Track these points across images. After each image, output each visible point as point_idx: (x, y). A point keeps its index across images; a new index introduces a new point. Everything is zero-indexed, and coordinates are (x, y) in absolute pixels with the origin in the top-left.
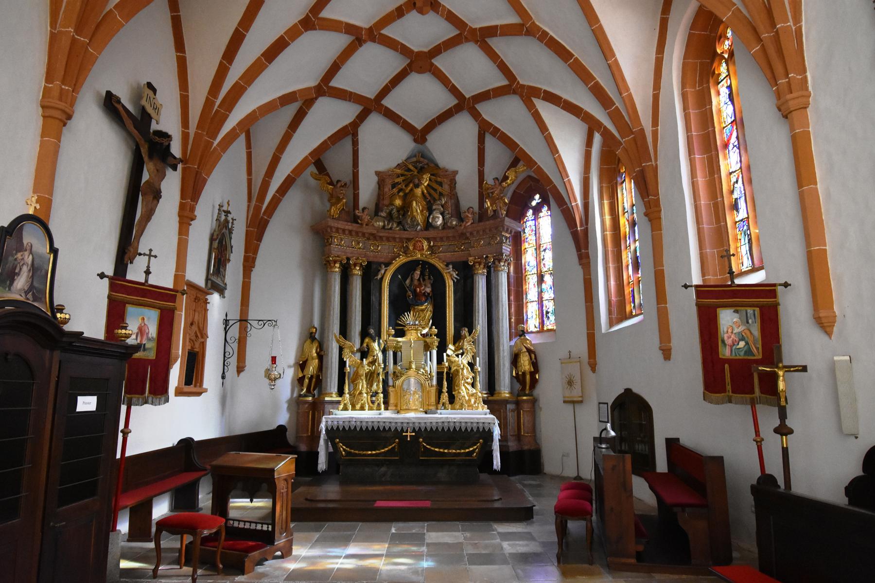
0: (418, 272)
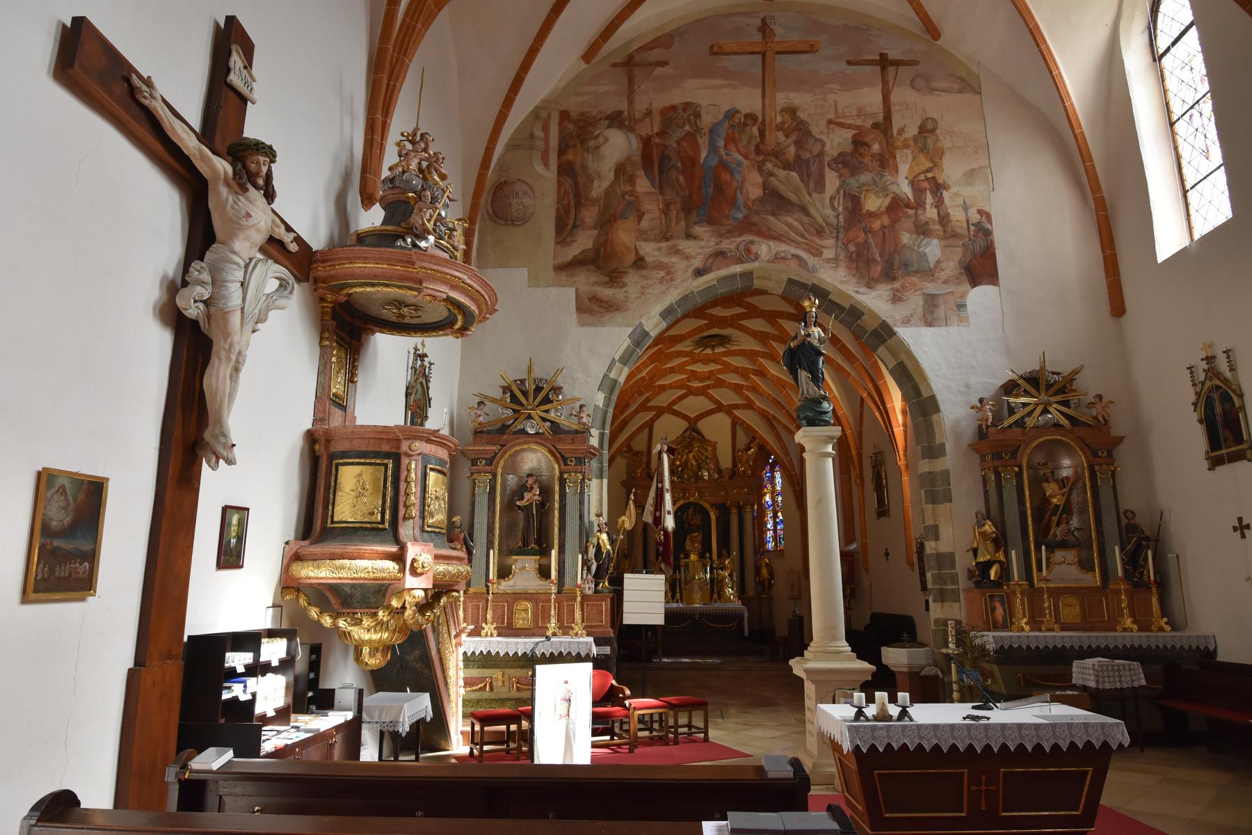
0: (691, 510)
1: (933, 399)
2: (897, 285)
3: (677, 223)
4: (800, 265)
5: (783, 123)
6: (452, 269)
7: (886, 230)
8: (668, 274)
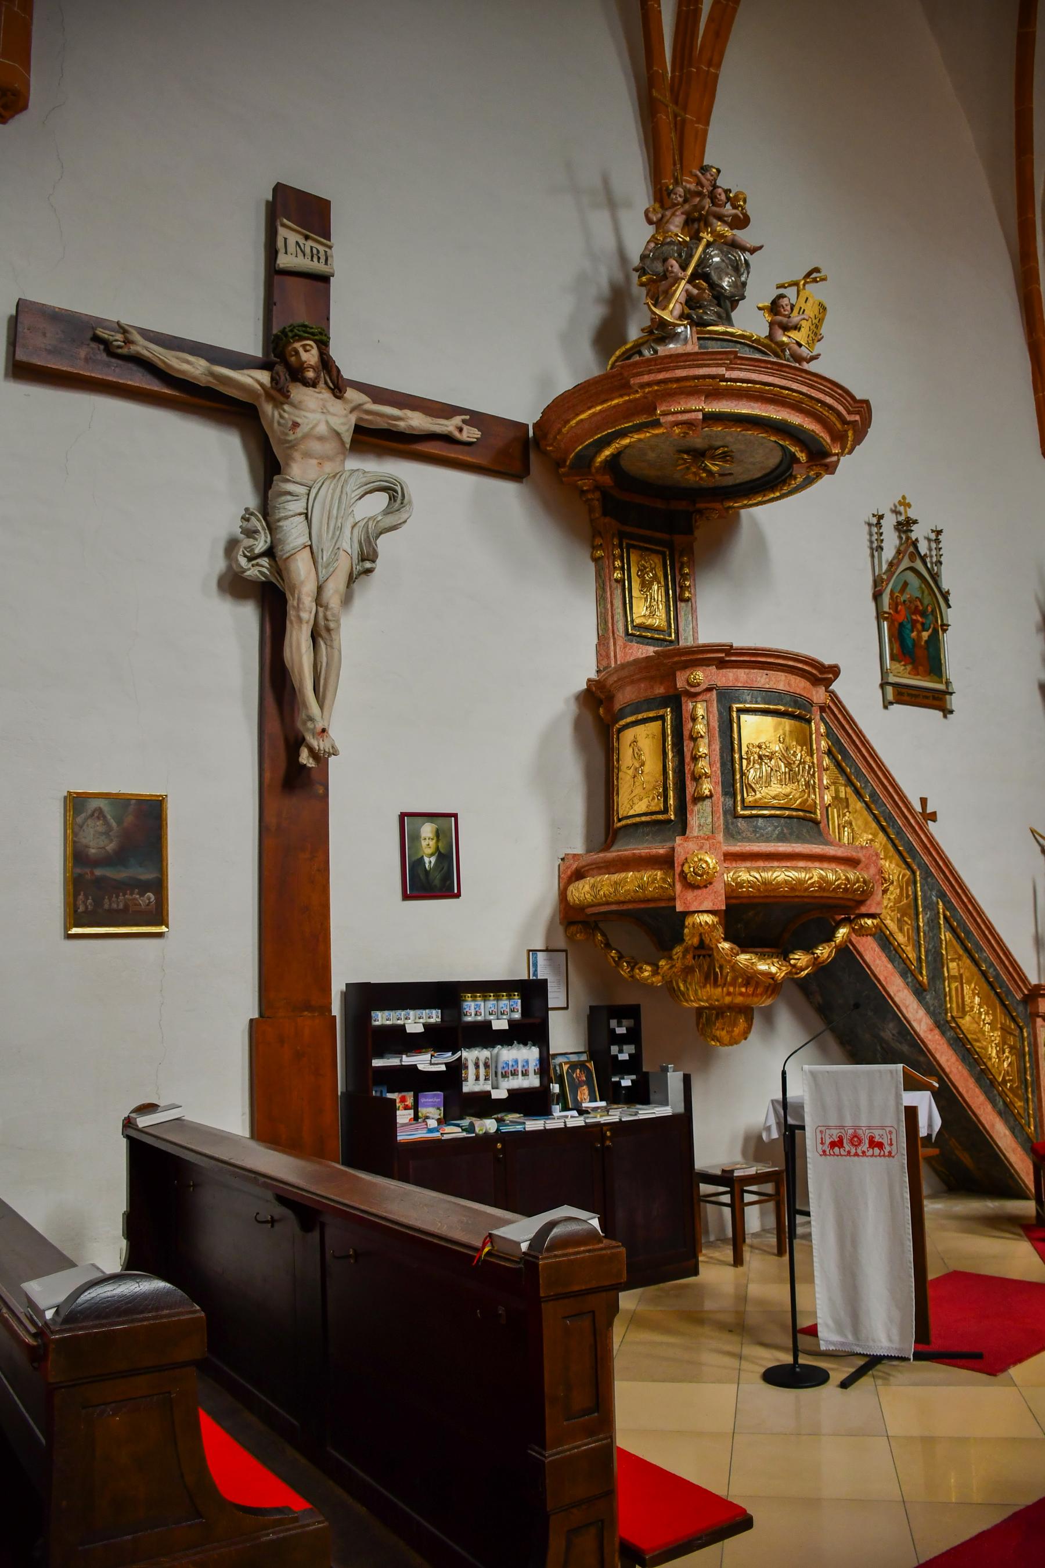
6: (690, 367)
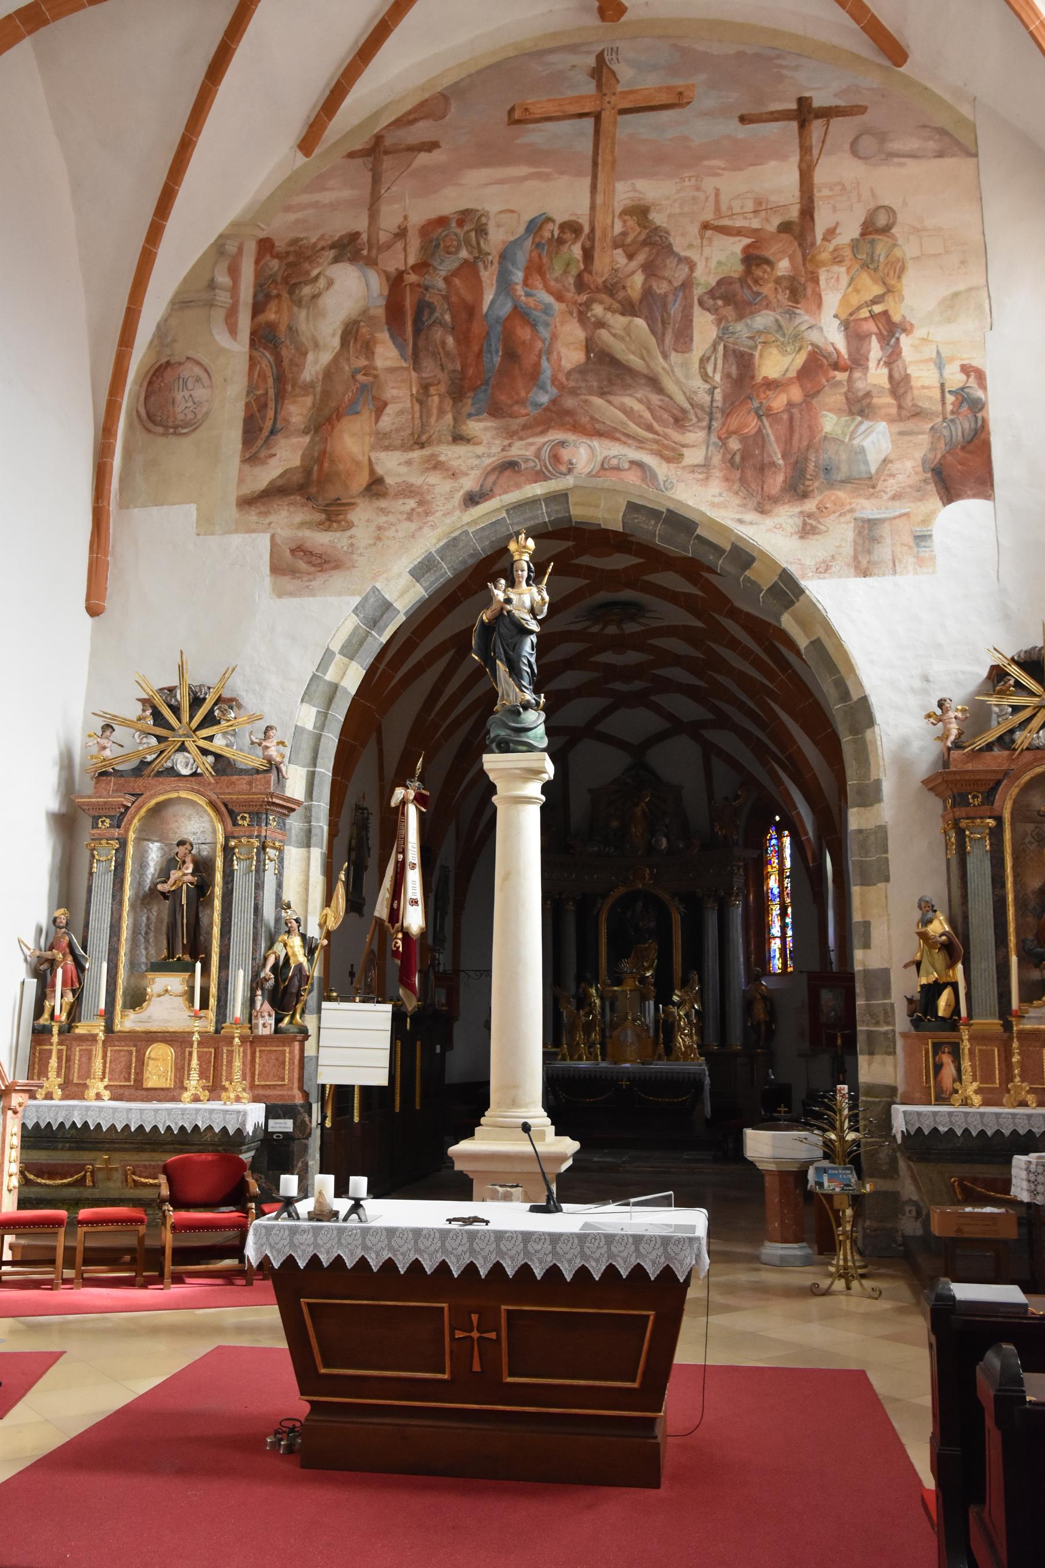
1: (864, 700)
2: (810, 505)
3: (441, 412)
4: (644, 480)
5: (624, 234)
7: (795, 411)
8: (421, 503)
